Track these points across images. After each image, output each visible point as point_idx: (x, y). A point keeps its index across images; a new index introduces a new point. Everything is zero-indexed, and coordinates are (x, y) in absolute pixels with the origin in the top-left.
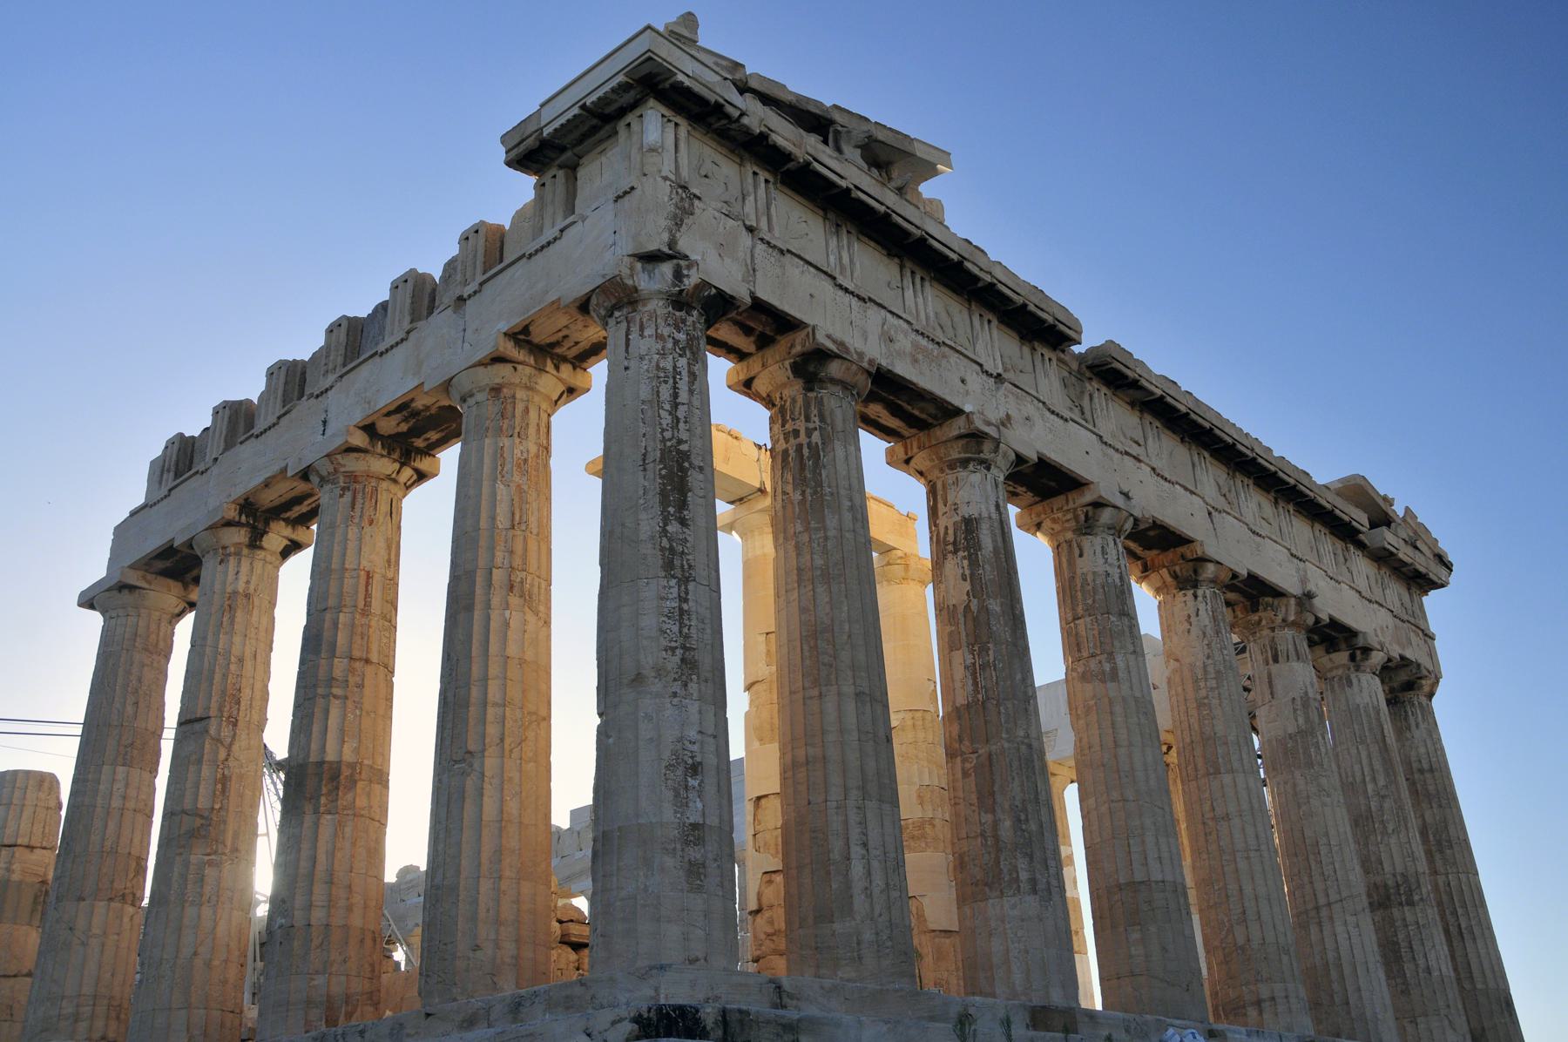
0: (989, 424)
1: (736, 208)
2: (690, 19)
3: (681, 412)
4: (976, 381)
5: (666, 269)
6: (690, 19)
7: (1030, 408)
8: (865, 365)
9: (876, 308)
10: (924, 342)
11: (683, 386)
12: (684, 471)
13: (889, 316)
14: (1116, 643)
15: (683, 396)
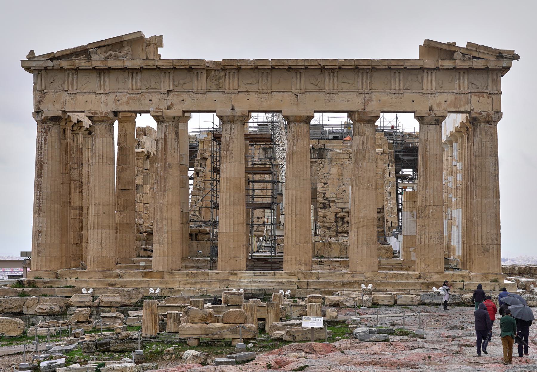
0: (157, 112)
1: (61, 88)
2: (32, 52)
3: (42, 151)
4: (156, 98)
5: (40, 114)
6: (32, 52)
7: (184, 96)
8: (103, 115)
9: (113, 94)
10: (134, 95)
11: (43, 144)
12: (42, 165)
13: (119, 94)
14: (225, 160)
15: (43, 147)
